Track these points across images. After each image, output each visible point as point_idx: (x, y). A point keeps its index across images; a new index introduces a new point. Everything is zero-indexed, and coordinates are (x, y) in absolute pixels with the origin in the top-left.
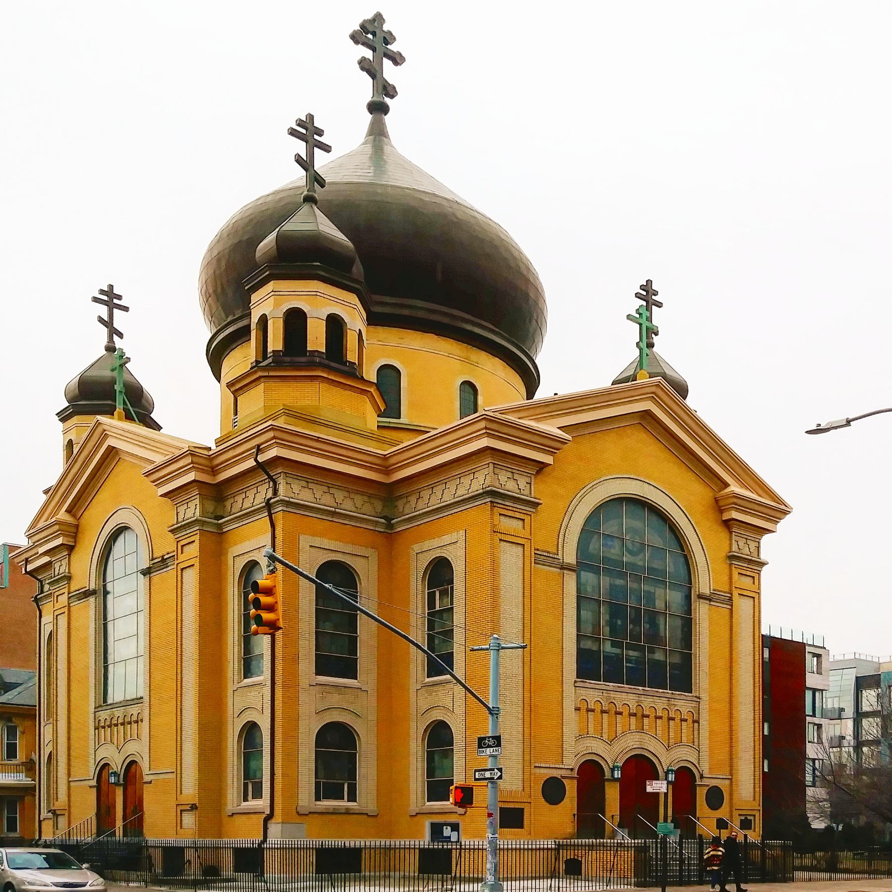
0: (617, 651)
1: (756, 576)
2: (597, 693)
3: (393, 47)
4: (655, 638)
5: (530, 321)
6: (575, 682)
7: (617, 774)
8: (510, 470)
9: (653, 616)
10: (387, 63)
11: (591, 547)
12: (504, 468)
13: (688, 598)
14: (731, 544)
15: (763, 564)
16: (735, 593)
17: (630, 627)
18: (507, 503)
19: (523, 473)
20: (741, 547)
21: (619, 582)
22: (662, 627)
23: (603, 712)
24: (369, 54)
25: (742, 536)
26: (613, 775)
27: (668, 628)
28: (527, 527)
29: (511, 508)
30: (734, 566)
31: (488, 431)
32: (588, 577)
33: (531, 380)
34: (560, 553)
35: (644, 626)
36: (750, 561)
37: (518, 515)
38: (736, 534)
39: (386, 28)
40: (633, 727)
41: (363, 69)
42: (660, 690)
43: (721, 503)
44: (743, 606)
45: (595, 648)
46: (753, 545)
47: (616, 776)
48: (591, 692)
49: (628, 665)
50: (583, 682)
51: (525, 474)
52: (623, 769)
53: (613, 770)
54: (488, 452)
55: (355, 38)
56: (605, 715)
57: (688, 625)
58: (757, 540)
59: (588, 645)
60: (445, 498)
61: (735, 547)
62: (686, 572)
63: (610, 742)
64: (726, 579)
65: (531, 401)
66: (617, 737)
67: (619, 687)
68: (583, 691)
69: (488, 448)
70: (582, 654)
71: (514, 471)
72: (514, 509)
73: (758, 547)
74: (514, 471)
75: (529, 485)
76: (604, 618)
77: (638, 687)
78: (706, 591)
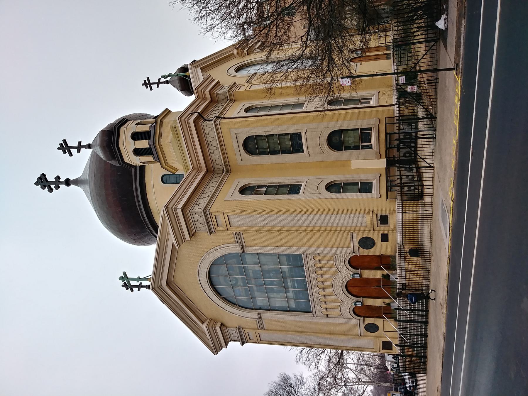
18: (244, 338)
19: (228, 332)
29: (246, 337)
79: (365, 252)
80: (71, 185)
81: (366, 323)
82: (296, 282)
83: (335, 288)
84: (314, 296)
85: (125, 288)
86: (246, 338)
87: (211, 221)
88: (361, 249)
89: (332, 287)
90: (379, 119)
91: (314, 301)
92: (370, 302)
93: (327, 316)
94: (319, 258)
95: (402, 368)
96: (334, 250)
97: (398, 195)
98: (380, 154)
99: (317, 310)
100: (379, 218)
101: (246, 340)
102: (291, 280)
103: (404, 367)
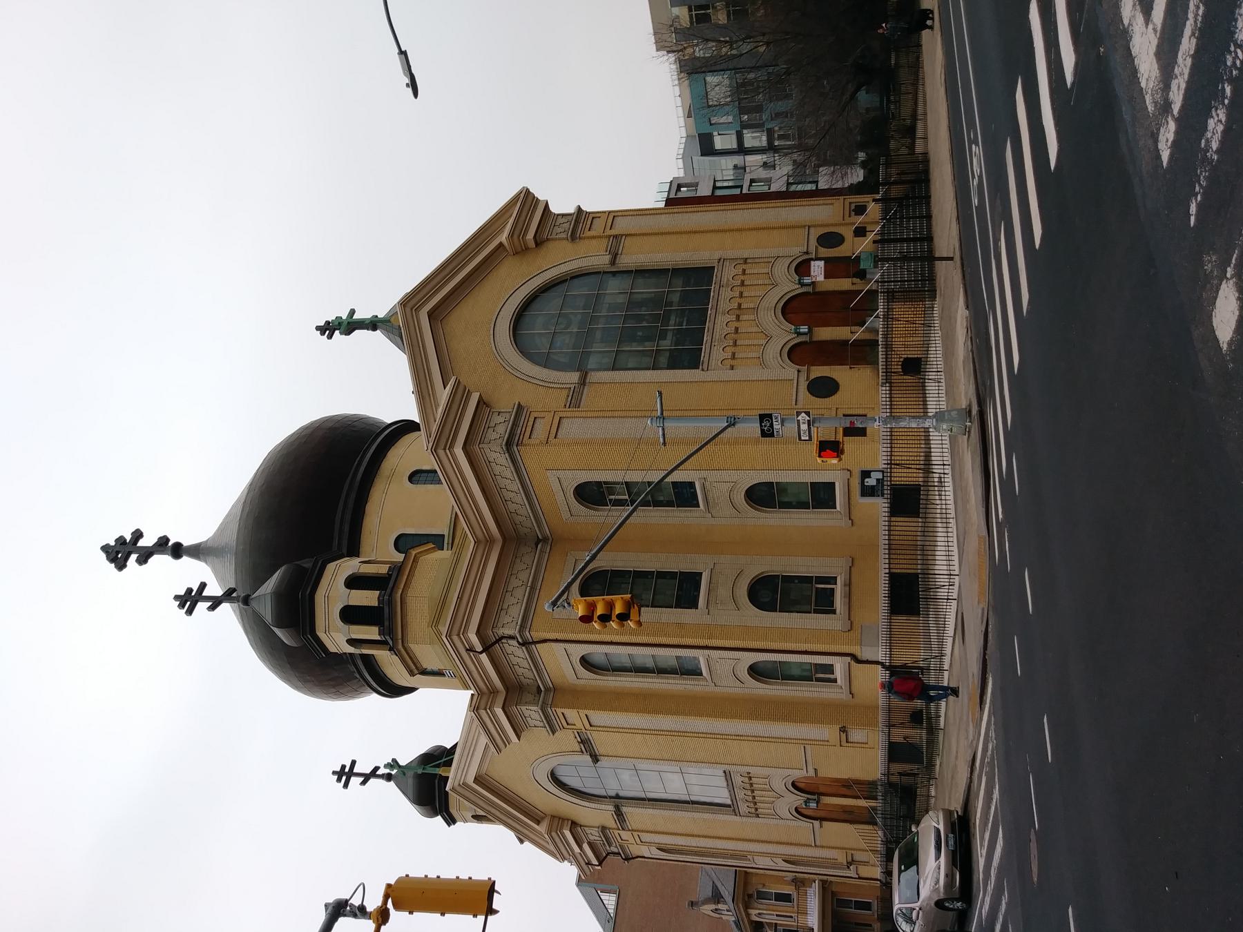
0: (670, 335)
1: (591, 216)
2: (715, 350)
3: (128, 538)
4: (657, 301)
5: (354, 427)
6: (703, 370)
7: (804, 329)
9: (631, 304)
10: (141, 543)
11: (562, 360)
12: (484, 435)
13: (614, 274)
14: (560, 239)
15: (579, 209)
16: (608, 232)
17: (645, 324)
18: (519, 432)
19: (489, 419)
21: (598, 335)
22: (645, 296)
23: (735, 344)
24: (134, 557)
25: (551, 230)
26: (805, 334)
27: (645, 289)
28: (542, 415)
29: (524, 429)
30: (581, 235)
31: (448, 448)
32: (592, 362)
33: (405, 427)
34: (568, 386)
35: (643, 311)
36: (577, 222)
37: (530, 423)
38: (549, 234)
39: (113, 543)
40: (752, 317)
41: (145, 561)
42: (712, 294)
43: (520, 250)
44: (621, 226)
45: (667, 354)
46: (560, 220)
47: (806, 330)
49: (685, 324)
50: (703, 363)
51: (490, 417)
52: (797, 325)
53: (799, 334)
54: (468, 447)
55: (121, 566)
57: (640, 273)
58: (556, 216)
59: (663, 360)
60: (515, 489)
61: (563, 235)
62: (586, 277)
63: (769, 338)
64: (594, 242)
65: (421, 425)
67: (708, 331)
68: (713, 363)
69: (465, 448)
70: (674, 364)
71: (487, 426)
72: (525, 426)
73: (563, 215)
74: (487, 426)
75: (501, 414)
76: (636, 347)
77: (708, 315)
78: (607, 259)
80: (182, 556)
81: (812, 376)
82: (685, 319)
83: (761, 314)
84: (715, 331)
85: (182, 593)
86: (523, 433)
88: (819, 247)
89: (756, 310)
90: (852, 559)
91: (713, 340)
92: (826, 333)
93: (732, 368)
94: (744, 267)
95: (886, 294)
96: (775, 252)
97: (884, 514)
99: (718, 327)
100: (853, 207)
101: (522, 436)
102: (675, 331)
103: (890, 292)
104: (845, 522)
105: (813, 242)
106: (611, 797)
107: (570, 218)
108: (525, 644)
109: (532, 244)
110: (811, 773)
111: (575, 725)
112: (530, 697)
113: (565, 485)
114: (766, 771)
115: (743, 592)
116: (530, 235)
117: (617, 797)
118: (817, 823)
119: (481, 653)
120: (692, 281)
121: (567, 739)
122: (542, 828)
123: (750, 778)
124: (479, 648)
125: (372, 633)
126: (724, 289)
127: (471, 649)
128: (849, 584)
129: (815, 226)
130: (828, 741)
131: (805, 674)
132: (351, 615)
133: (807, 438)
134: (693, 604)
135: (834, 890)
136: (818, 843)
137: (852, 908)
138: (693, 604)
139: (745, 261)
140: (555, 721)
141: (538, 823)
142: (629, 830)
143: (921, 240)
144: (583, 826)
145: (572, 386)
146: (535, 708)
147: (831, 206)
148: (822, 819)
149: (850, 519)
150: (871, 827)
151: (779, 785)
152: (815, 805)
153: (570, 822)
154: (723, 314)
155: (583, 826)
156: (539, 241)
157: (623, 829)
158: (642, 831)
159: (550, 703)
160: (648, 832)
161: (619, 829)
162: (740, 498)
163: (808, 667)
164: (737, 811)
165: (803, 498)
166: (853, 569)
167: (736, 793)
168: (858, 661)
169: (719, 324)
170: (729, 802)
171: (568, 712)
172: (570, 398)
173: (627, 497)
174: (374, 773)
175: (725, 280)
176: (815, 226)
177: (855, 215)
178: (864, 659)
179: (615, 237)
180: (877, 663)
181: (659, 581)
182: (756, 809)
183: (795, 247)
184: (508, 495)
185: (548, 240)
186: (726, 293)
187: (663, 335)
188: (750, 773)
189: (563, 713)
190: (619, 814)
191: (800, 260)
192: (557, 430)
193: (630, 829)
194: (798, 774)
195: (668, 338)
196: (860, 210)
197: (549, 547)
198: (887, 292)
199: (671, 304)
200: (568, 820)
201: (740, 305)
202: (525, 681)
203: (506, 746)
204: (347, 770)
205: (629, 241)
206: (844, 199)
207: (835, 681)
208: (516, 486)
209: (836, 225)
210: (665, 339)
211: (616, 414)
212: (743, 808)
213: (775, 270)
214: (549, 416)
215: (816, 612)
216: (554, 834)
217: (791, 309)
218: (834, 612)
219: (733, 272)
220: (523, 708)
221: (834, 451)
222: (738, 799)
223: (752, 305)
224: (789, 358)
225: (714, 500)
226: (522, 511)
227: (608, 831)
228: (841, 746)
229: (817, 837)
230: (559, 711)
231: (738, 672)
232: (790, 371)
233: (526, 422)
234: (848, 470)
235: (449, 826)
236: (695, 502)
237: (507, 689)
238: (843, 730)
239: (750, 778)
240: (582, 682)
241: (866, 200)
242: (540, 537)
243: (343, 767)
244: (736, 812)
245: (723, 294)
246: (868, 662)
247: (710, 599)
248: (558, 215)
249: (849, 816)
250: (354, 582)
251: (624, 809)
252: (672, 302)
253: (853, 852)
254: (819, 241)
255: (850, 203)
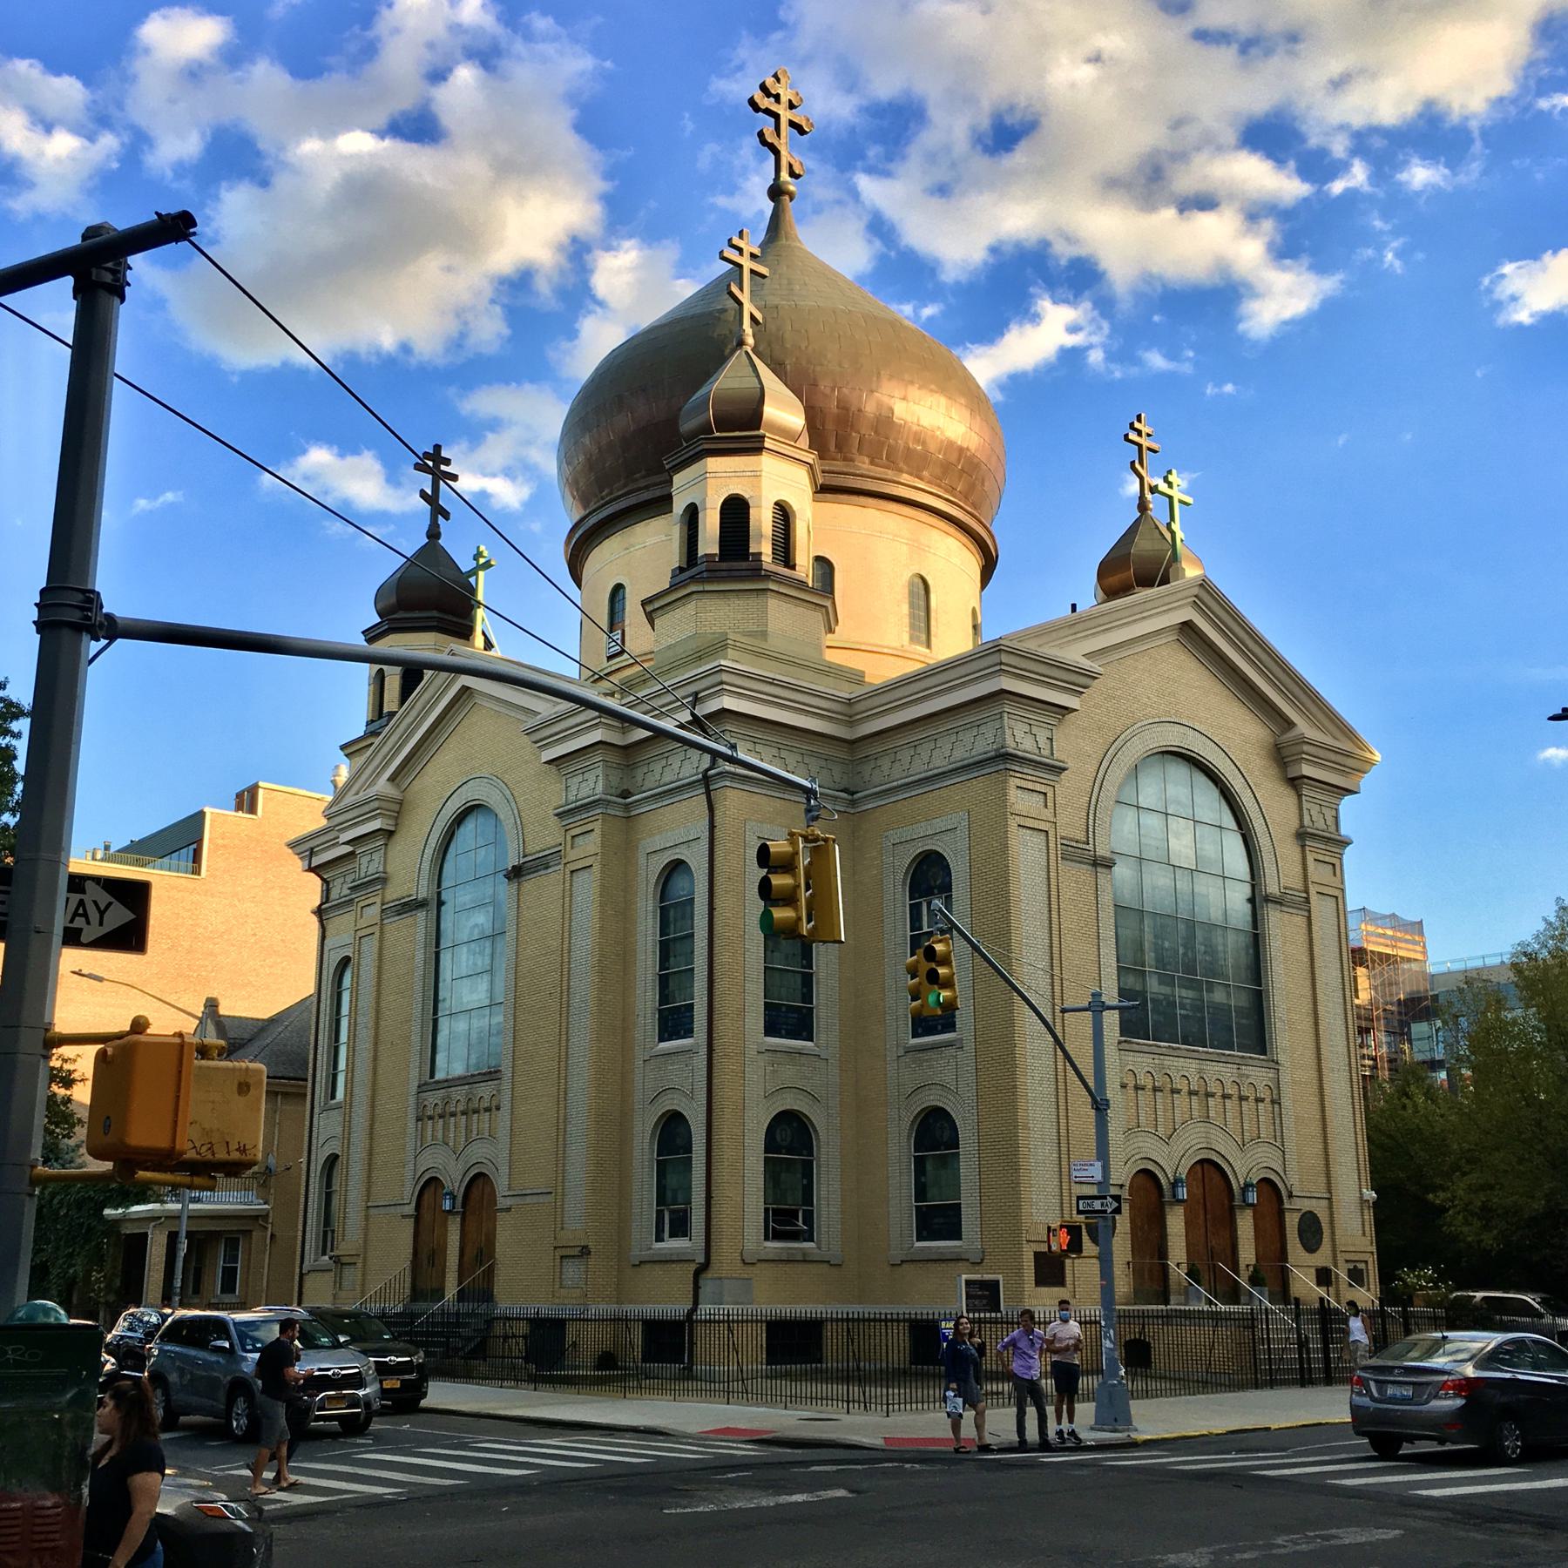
0: (1166, 990)
6: (1120, 1043)
7: (1183, 1193)
8: (1026, 720)
15: (1345, 843)
16: (1313, 890)
18: (1025, 771)
19: (1042, 724)
20: (1316, 819)
25: (1315, 801)
26: (1174, 1195)
29: (1030, 778)
38: (1308, 798)
44: (1322, 909)
45: (1138, 987)
48: (1139, 1058)
49: (1183, 1012)
56: (1158, 1094)
57: (1257, 941)
58: (1334, 806)
59: (1131, 982)
63: (1167, 1140)
64: (1298, 869)
66: (1175, 1130)
68: (1130, 1057)
71: (1031, 722)
73: (1336, 818)
74: (1031, 722)
76: (1148, 938)
79: (1292, 1221)
86: (1024, 776)
87: (1328, 848)
91: (1162, 1057)
92: (1176, 1223)
93: (1124, 1086)
95: (1250, 1317)
96: (1290, 1146)
98: (639, 1265)
100: (1361, 1266)
103: (1253, 1323)
104: (897, 1254)
105: (1306, 1205)
106: (439, 894)
107: (1332, 829)
108: (706, 780)
109: (1292, 773)
110: (502, 1203)
111: (572, 848)
112: (615, 781)
113: (945, 837)
114: (503, 1132)
115: (789, 1102)
116: (1307, 770)
117: (441, 903)
118: (410, 1209)
119: (693, 714)
120: (1244, 1021)
121: (544, 836)
122: (382, 786)
123: (488, 1110)
124: (701, 711)
125: (709, 542)
126: (1235, 1071)
127: (696, 699)
128: (806, 1260)
129: (1331, 1207)
130: (562, 1228)
131: (669, 1194)
132: (736, 511)
133: (1081, 1208)
134: (771, 1029)
135: (254, 1233)
136: (372, 1211)
137: (224, 1262)
138: (771, 1029)
139: (1276, 1102)
140: (579, 818)
141: (392, 779)
142: (382, 920)
143: (1327, 1369)
144: (386, 849)
145: (1090, 847)
146: (600, 788)
147: (1361, 1232)
148: (417, 1219)
149: (902, 1261)
150: (408, 1292)
151: (478, 1152)
152: (448, 1208)
153: (392, 829)
154: (1200, 1071)
155: (386, 849)
156: (1296, 782)
157: (383, 910)
158: (381, 940)
159: (609, 811)
160: (381, 949)
161: (383, 905)
162: (932, 1099)
163: (680, 1198)
164: (424, 1088)
165: (932, 1192)
166: (825, 1265)
167: (459, 1088)
168: (697, 1274)
169: (1185, 1066)
170: (439, 1076)
171: (596, 837)
172: (1074, 844)
173: (926, 929)
174: (438, 511)
175: (1245, 1070)
176: (1331, 1207)
177: (1349, 1270)
178: (701, 1283)
179: (1307, 900)
180: (696, 1302)
181: (799, 978)
182: (431, 1118)
183: (1301, 1182)
184: (924, 751)
185: (1300, 796)
186: (1227, 1072)
187: (1166, 980)
188: (498, 1108)
189: (593, 830)
190: (409, 906)
191: (1280, 1185)
192: (1030, 828)
193: (385, 922)
194: (501, 1184)
195: (1162, 987)
196: (1357, 1276)
197: (842, 809)
198: (1253, 1319)
199: (1210, 990)
200: (396, 825)
201: (1213, 1095)
202: (639, 773)
203: (536, 742)
204: (443, 468)
205: (1300, 921)
206: (1372, 1253)
207: (659, 1239)
208: (940, 763)
209: (1333, 1241)
210: (1160, 984)
211: (1055, 916)
212: (433, 1098)
213: (1266, 1148)
214: (1047, 814)
215: (766, 1210)
216: (375, 804)
217: (1209, 1169)
218: (767, 1238)
219: (1261, 1087)
220: (599, 771)
221: (1068, 1245)
222: (450, 1090)
223: (1212, 1113)
224: (1139, 1172)
225: (927, 1061)
226: (897, 771)
227: (379, 887)
228: (555, 1248)
229: (382, 1210)
230: (597, 826)
231: (670, 1096)
232: (1121, 1174)
233: (1038, 779)
234: (982, 1260)
235: (363, 632)
236: (920, 1031)
237: (626, 747)
238: (585, 1252)
239: (488, 1110)
240: (642, 860)
241: (1372, 1286)
242: (855, 796)
243: (447, 462)
244: (422, 1088)
245: (1228, 1070)
246: (696, 1288)
247: (779, 1055)
248: (1337, 810)
249: (425, 1258)
250: (784, 513)
251: (421, 915)
252: (1213, 992)
253: (359, 1265)
254: (1308, 1215)
255: (1366, 1262)
